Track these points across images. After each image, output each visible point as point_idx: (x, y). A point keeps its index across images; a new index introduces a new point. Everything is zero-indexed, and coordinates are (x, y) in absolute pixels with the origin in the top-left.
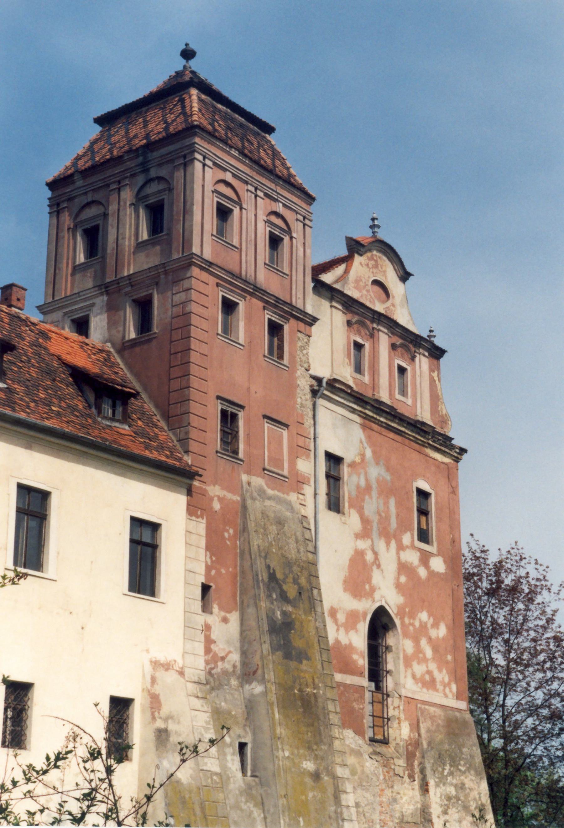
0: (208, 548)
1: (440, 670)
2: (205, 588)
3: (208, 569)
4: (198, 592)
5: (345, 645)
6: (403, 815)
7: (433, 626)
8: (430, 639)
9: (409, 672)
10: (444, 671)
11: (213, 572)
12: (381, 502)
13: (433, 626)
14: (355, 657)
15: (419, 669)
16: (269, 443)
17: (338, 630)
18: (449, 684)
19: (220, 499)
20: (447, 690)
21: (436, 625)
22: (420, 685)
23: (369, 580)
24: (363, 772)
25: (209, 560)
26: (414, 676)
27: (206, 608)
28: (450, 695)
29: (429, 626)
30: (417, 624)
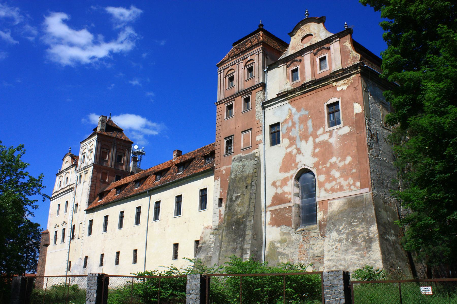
0: (221, 187)
1: (346, 180)
2: (221, 200)
3: (221, 193)
4: (217, 202)
5: (281, 193)
6: (314, 254)
7: (340, 162)
8: (339, 169)
9: (323, 189)
10: (350, 178)
11: (223, 193)
12: (302, 126)
13: (340, 162)
14: (286, 196)
15: (328, 186)
16: (244, 139)
17: (277, 189)
18: (354, 184)
19: (225, 170)
20: (352, 187)
21: (344, 159)
22: (330, 192)
23: (294, 161)
24: (290, 240)
25: (221, 191)
26: (326, 190)
27: (220, 205)
28: (356, 189)
29: (337, 162)
30: (328, 165)
